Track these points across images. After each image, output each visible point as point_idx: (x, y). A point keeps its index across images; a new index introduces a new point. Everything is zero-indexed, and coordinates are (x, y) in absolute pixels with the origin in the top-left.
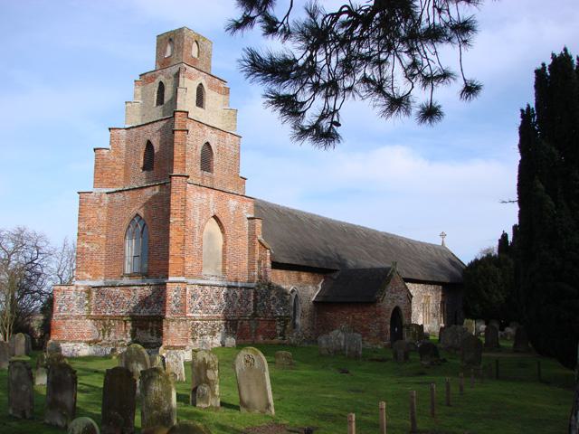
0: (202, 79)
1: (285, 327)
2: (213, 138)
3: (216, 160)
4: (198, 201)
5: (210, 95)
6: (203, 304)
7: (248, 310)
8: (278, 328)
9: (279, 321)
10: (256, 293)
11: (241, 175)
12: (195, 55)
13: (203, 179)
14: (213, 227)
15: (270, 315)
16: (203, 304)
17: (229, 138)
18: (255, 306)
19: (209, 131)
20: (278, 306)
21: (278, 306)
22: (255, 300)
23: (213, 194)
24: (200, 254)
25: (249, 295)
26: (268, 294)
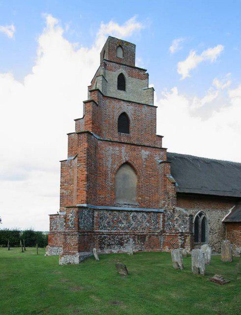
0: (122, 70)
1: (185, 240)
2: (129, 110)
3: (132, 125)
4: (111, 152)
5: (130, 83)
6: (111, 223)
7: (159, 228)
8: (180, 241)
9: (180, 236)
10: (164, 216)
11: (157, 134)
12: (121, 57)
13: (120, 138)
14: (127, 171)
15: (174, 231)
16: (111, 223)
17: (145, 109)
18: (164, 226)
19: (125, 105)
20: (180, 226)
21: (180, 226)
22: (164, 221)
23: (124, 148)
24: (113, 190)
25: (158, 217)
26: (172, 216)
